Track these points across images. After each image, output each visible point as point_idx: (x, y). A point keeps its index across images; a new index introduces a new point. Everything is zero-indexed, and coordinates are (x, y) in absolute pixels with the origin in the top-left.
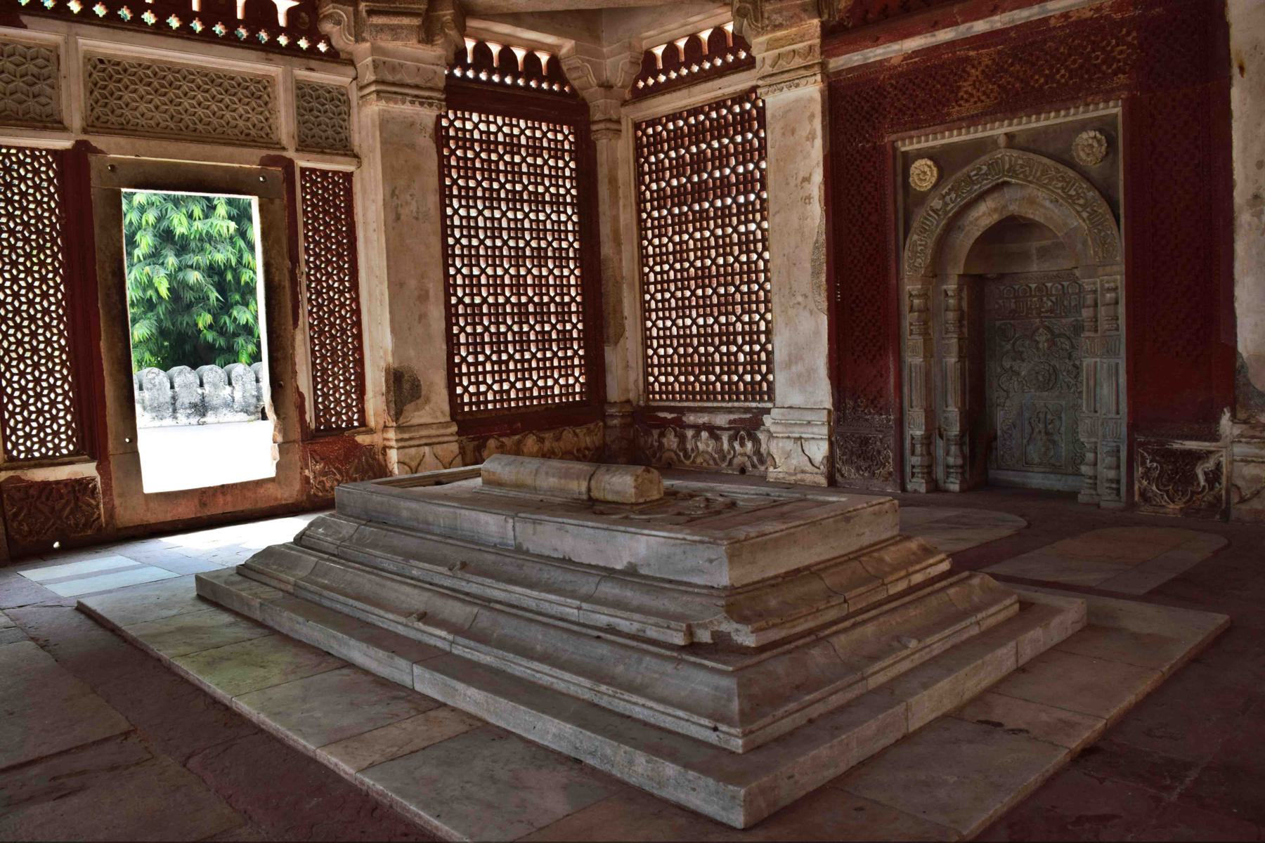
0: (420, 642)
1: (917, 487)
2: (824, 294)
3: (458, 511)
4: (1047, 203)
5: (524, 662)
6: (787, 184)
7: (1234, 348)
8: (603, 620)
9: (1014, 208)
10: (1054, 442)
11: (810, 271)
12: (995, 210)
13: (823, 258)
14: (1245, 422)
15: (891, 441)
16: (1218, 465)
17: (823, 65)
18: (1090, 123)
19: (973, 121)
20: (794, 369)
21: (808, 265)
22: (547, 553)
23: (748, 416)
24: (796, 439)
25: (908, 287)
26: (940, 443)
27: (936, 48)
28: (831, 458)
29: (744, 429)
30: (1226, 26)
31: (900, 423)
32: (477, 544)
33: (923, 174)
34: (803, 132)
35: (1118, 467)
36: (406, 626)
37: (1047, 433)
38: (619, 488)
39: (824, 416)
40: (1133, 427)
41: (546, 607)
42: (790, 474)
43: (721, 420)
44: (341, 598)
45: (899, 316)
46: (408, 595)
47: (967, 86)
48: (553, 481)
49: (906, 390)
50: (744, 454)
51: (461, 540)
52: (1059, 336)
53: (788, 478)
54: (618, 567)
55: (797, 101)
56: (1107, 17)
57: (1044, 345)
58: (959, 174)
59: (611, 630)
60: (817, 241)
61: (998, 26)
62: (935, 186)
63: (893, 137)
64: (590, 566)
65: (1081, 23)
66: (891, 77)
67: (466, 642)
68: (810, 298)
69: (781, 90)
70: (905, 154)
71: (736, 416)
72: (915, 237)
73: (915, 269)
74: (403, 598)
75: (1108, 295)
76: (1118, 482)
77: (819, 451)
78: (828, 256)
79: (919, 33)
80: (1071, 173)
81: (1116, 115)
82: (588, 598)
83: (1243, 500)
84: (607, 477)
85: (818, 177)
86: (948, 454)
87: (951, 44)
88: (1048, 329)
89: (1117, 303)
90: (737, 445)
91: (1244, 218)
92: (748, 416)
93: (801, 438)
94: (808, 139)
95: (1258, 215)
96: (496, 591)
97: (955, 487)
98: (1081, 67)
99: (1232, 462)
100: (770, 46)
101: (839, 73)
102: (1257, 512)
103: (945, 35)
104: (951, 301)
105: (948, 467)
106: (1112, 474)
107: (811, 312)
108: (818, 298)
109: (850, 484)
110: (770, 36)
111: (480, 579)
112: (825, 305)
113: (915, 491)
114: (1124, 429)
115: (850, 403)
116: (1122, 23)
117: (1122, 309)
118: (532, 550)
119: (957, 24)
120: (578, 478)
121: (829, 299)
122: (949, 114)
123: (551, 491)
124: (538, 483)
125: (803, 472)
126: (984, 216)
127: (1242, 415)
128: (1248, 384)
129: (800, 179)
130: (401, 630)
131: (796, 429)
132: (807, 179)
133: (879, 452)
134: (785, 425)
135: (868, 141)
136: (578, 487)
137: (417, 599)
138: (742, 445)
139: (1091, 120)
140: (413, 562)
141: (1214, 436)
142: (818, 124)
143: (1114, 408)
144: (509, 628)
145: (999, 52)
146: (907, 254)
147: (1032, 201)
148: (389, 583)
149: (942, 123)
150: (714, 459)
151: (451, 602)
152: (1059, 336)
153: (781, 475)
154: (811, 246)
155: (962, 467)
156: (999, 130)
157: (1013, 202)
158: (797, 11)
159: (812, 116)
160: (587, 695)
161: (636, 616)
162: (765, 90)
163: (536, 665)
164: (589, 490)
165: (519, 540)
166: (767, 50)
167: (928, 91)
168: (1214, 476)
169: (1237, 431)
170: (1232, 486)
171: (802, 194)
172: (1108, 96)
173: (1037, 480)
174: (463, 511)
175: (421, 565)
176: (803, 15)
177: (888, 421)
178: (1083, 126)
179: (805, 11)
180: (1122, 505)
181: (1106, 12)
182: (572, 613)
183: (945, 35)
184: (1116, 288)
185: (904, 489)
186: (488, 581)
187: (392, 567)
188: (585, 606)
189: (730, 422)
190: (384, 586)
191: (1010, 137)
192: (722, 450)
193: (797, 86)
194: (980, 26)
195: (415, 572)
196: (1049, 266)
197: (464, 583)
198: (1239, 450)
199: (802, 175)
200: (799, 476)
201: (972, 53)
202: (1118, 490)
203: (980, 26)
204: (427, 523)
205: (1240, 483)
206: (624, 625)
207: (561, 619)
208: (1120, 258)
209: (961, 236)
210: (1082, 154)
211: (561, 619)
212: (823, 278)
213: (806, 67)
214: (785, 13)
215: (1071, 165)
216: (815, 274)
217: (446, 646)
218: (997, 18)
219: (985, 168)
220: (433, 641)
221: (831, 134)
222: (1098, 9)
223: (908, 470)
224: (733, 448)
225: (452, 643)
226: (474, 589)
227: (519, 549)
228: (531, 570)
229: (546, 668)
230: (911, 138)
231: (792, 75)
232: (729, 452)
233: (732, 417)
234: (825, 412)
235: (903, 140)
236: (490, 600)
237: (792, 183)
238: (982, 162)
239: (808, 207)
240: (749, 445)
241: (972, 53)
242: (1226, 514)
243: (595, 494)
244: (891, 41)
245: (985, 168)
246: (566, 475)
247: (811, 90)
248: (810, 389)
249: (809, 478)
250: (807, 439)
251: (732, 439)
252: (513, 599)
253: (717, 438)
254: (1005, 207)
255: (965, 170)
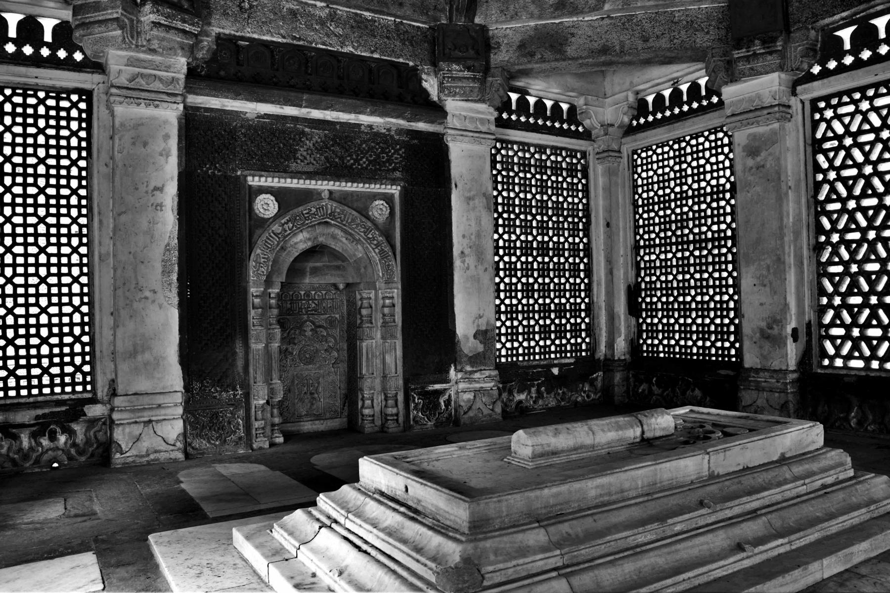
0: (768, 560)
1: (261, 445)
2: (175, 291)
3: (658, 467)
4: (344, 240)
5: (834, 522)
6: (137, 189)
7: (455, 332)
8: (818, 484)
9: (321, 239)
10: (314, 398)
11: (160, 270)
12: (309, 239)
13: (175, 259)
14: (461, 371)
15: (242, 412)
16: (450, 396)
17: (185, 98)
18: (385, 195)
19: (310, 176)
20: (139, 358)
21: (159, 267)
22: (731, 470)
23: (63, 409)
24: (145, 422)
25: (252, 290)
26: (269, 408)
27: (285, 118)
28: (185, 434)
29: (56, 423)
30: (448, 162)
31: (247, 396)
32: (676, 488)
33: (265, 206)
34: (158, 145)
35: (396, 405)
36: (748, 557)
37: (312, 394)
38: (664, 425)
39: (179, 398)
40: (406, 381)
41: (788, 494)
42: (142, 456)
43: (25, 417)
44: (669, 581)
45: (245, 313)
46: (707, 543)
47: (302, 151)
48: (612, 435)
49: (251, 371)
50: (57, 448)
51: (670, 489)
52: (320, 326)
53: (138, 460)
54: (775, 459)
55: (153, 118)
56: (392, 137)
57: (309, 333)
58: (296, 211)
59: (824, 486)
60: (168, 244)
61: (329, 118)
62: (277, 217)
63: (246, 172)
64: (760, 466)
65: (378, 134)
66: (242, 127)
67: (797, 535)
68: (160, 297)
69: (139, 104)
70: (250, 186)
71: (40, 412)
72: (259, 251)
73: (258, 275)
74: (705, 547)
75: (387, 301)
76: (397, 415)
77: (174, 429)
78: (180, 258)
79: (272, 103)
80: (369, 224)
81: (393, 195)
82: (796, 479)
83: (465, 413)
84: (653, 420)
85: (172, 189)
86: (272, 416)
87: (295, 119)
88: (313, 323)
89: (394, 306)
90: (45, 442)
91: (457, 263)
92: (63, 409)
93: (150, 421)
94: (161, 155)
95: (463, 262)
96: (772, 495)
97: (281, 440)
98: (375, 160)
99: (457, 393)
100: (131, 62)
101: (198, 109)
102: (471, 418)
103: (290, 111)
104: (273, 301)
105: (273, 425)
106: (394, 411)
107: (160, 307)
108: (168, 294)
109: (203, 454)
110: (132, 54)
111: (737, 502)
112: (176, 300)
113: (261, 448)
114: (401, 382)
115: (197, 385)
116: (397, 142)
117: (398, 309)
118: (721, 471)
119: (300, 106)
120: (632, 427)
121: (181, 294)
122: (288, 166)
123: (609, 444)
124: (597, 440)
125: (156, 452)
126: (301, 241)
127: (459, 368)
128: (461, 350)
129: (151, 187)
130: (747, 563)
131: (146, 414)
132: (160, 189)
133: (229, 423)
134: (132, 411)
135: (219, 171)
136: (633, 433)
137: (719, 540)
138: (53, 438)
139: (379, 194)
140: (670, 521)
141: (447, 381)
142: (173, 144)
143: (393, 370)
144: (792, 516)
145: (326, 136)
146: (252, 263)
147: (334, 237)
148: (678, 546)
149: (285, 171)
150: (13, 461)
151: (743, 525)
152: (320, 326)
153: (130, 459)
154: (163, 247)
155: (263, 428)
156: (324, 186)
157: (323, 236)
158: (177, 46)
159: (167, 137)
160: (868, 516)
161: (832, 472)
162: (117, 99)
163: (841, 519)
164: (643, 432)
165: (713, 468)
166: (127, 65)
167: (274, 146)
168: (448, 402)
169: (460, 375)
170: (458, 407)
171: (152, 200)
172: (394, 182)
173: (308, 426)
174: (664, 465)
175: (680, 518)
176: (179, 52)
177: (235, 395)
178: (375, 196)
179: (183, 49)
180: (401, 428)
181: (393, 133)
182: (803, 489)
183: (290, 111)
184: (392, 298)
185: (252, 449)
186: (744, 499)
187: (650, 537)
188: (807, 481)
189: (37, 417)
190: (677, 551)
191: (331, 192)
192: (21, 449)
193: (157, 106)
194: (316, 114)
195: (678, 528)
196: (316, 280)
197: (727, 512)
198: (462, 386)
199: (152, 185)
200: (152, 457)
201: (306, 129)
202: (397, 420)
203: (316, 114)
204: (622, 491)
205: (462, 404)
206: (829, 480)
207: (798, 497)
208: (397, 277)
209: (284, 254)
210: (376, 214)
211: (798, 497)
212: (175, 277)
213: (168, 94)
214: (165, 43)
215: (368, 218)
216: (166, 272)
217: (787, 548)
218: (327, 112)
219: (314, 210)
220: (775, 553)
221: (188, 154)
222: (389, 130)
223: (254, 432)
224: (39, 444)
225: (790, 542)
226: (737, 510)
227: (713, 477)
228: (748, 481)
229: (845, 517)
230: (261, 176)
231: (153, 96)
232: (31, 448)
233: (40, 412)
234: (180, 394)
235: (254, 176)
236: (755, 511)
237: (143, 188)
238: (312, 207)
239: (160, 213)
240: (62, 439)
241: (306, 129)
242: (457, 422)
243: (648, 435)
244: (247, 100)
245: (314, 210)
246: (619, 428)
247: (170, 115)
248: (159, 376)
249: (163, 456)
250: (158, 421)
251: (34, 436)
252: (767, 502)
253: (16, 437)
254: (315, 238)
255: (300, 209)
